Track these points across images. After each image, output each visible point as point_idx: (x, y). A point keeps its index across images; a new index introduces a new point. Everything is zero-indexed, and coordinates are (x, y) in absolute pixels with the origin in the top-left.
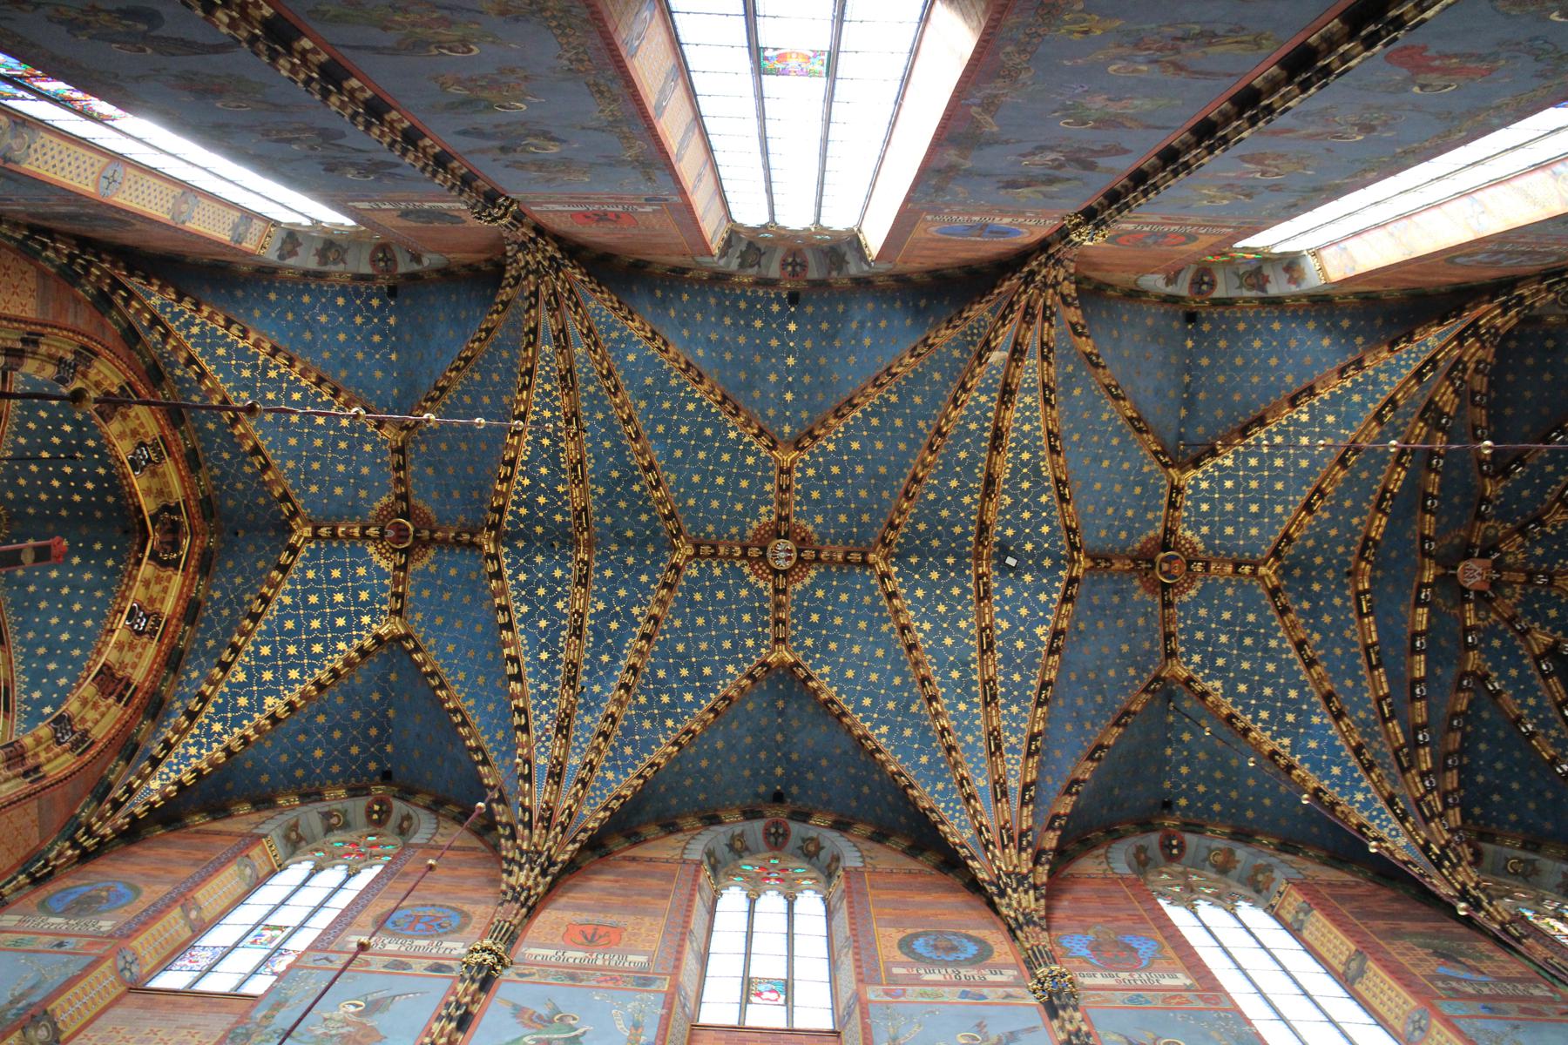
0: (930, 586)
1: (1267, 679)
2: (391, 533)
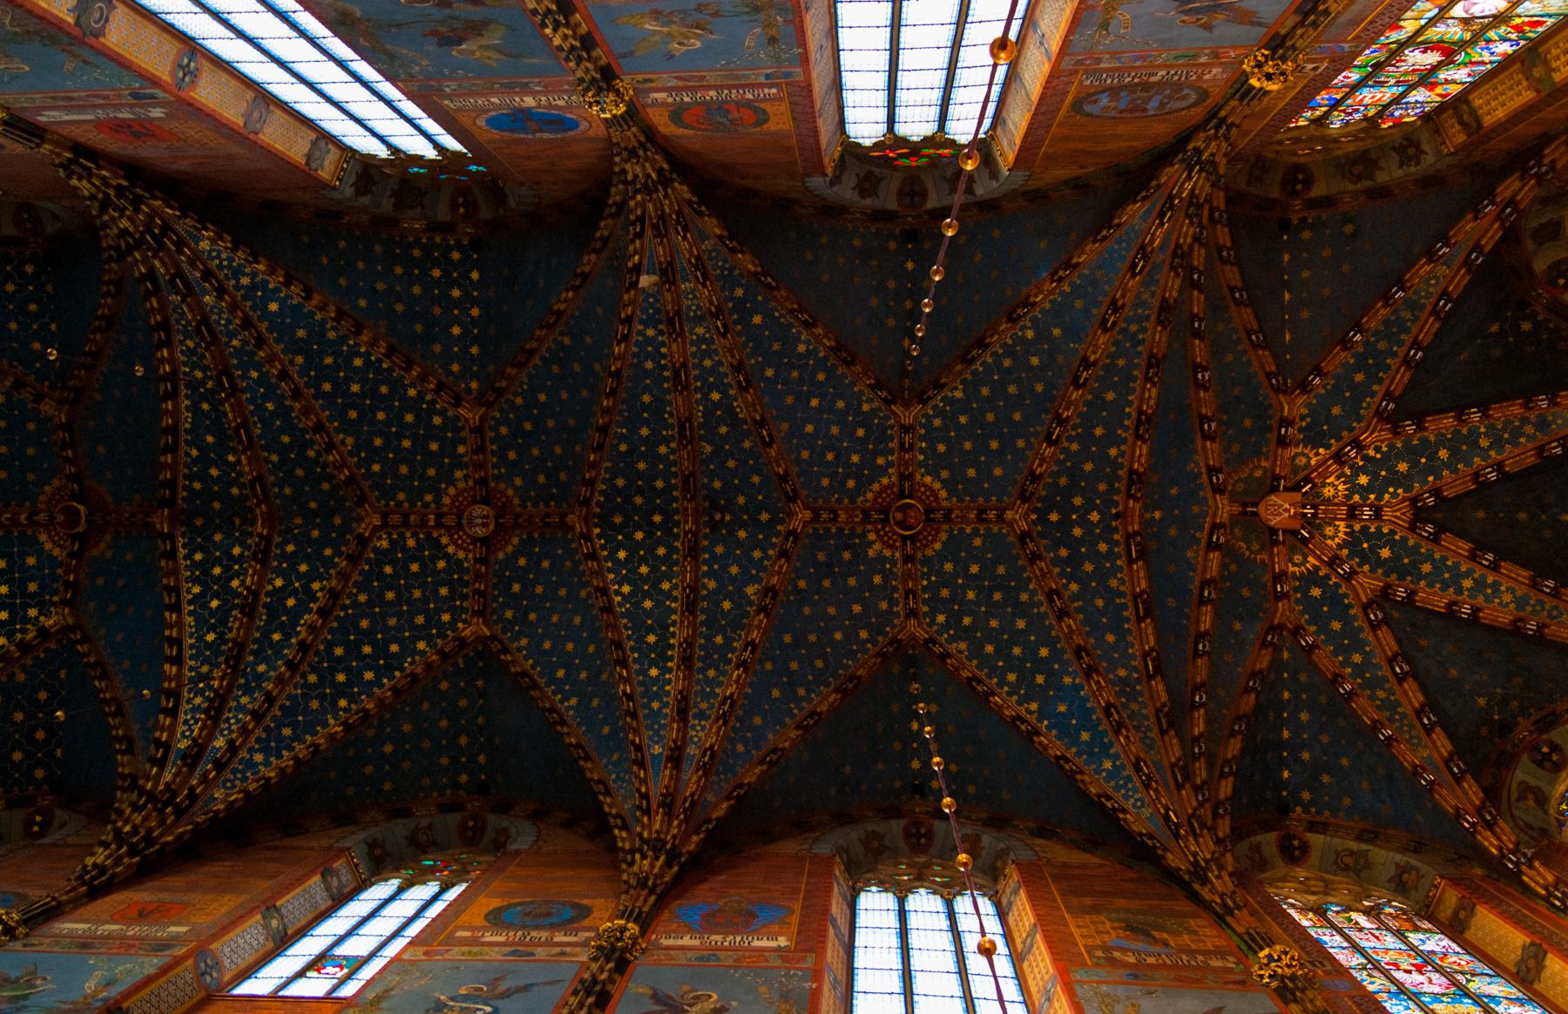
0: (632, 547)
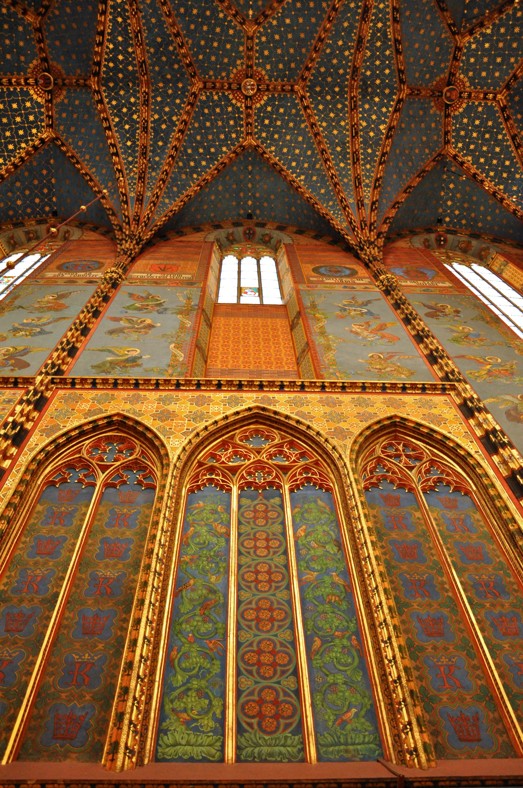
0: (326, 104)
1: (496, 155)
2: (41, 81)
